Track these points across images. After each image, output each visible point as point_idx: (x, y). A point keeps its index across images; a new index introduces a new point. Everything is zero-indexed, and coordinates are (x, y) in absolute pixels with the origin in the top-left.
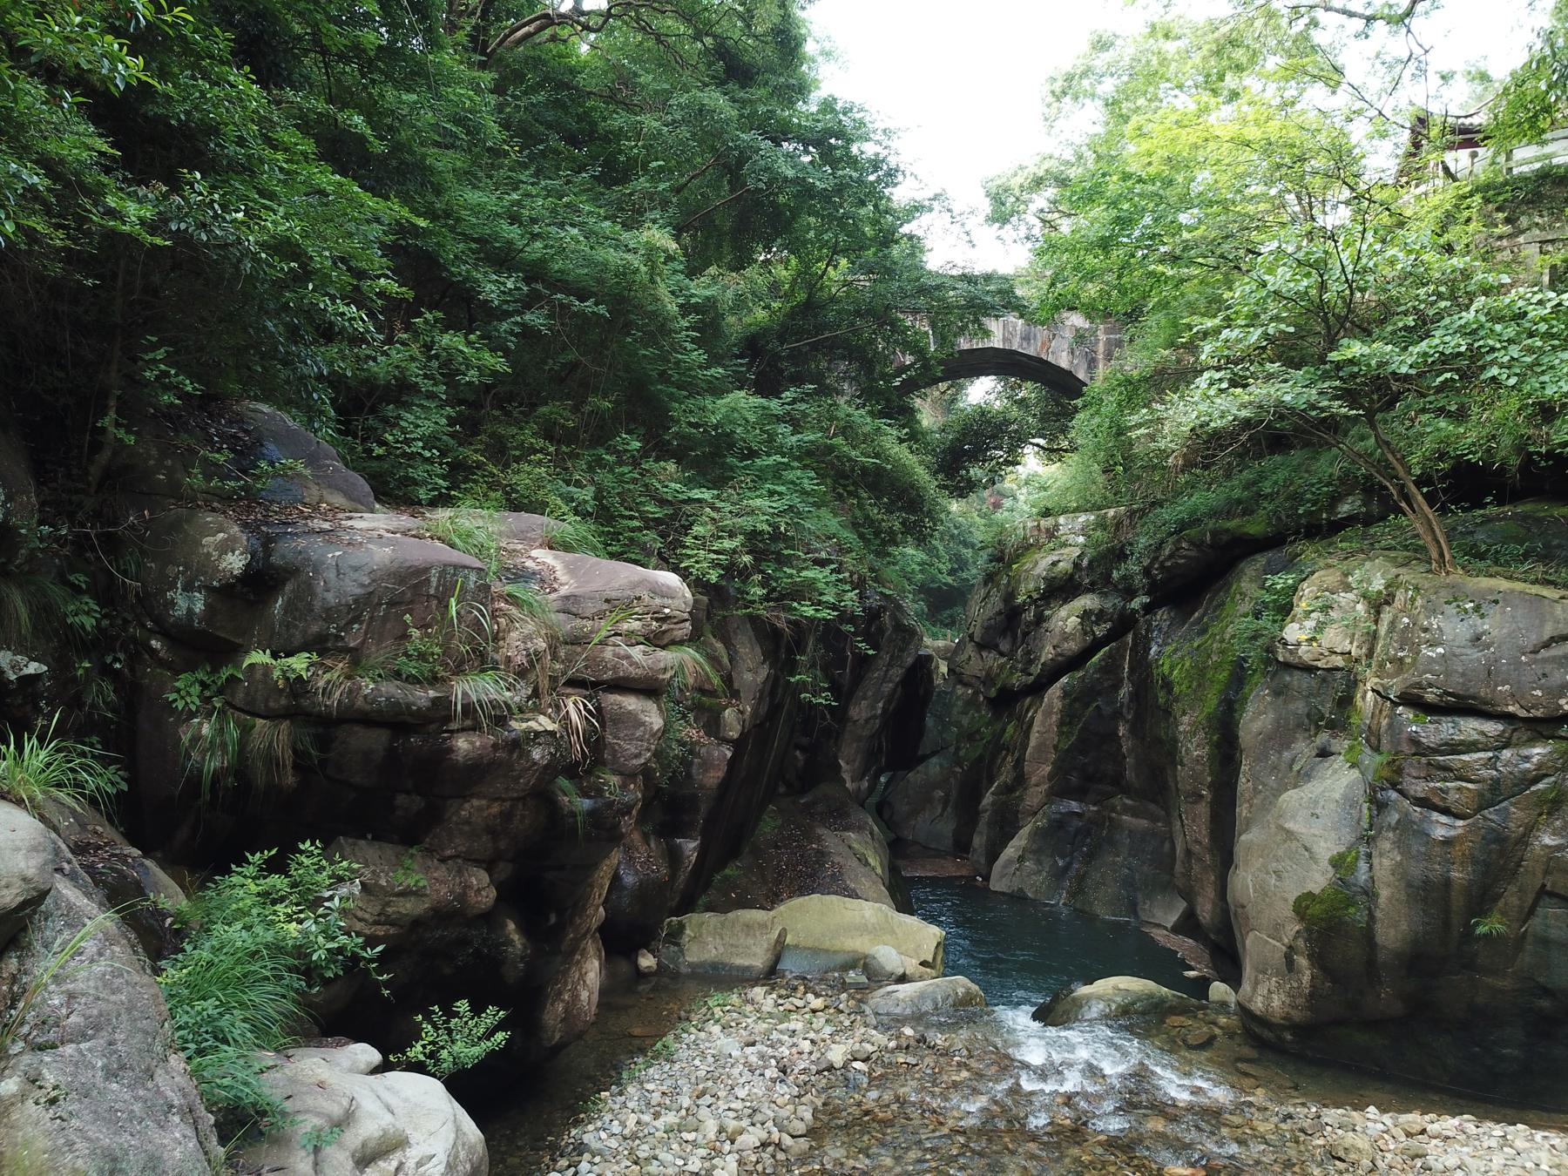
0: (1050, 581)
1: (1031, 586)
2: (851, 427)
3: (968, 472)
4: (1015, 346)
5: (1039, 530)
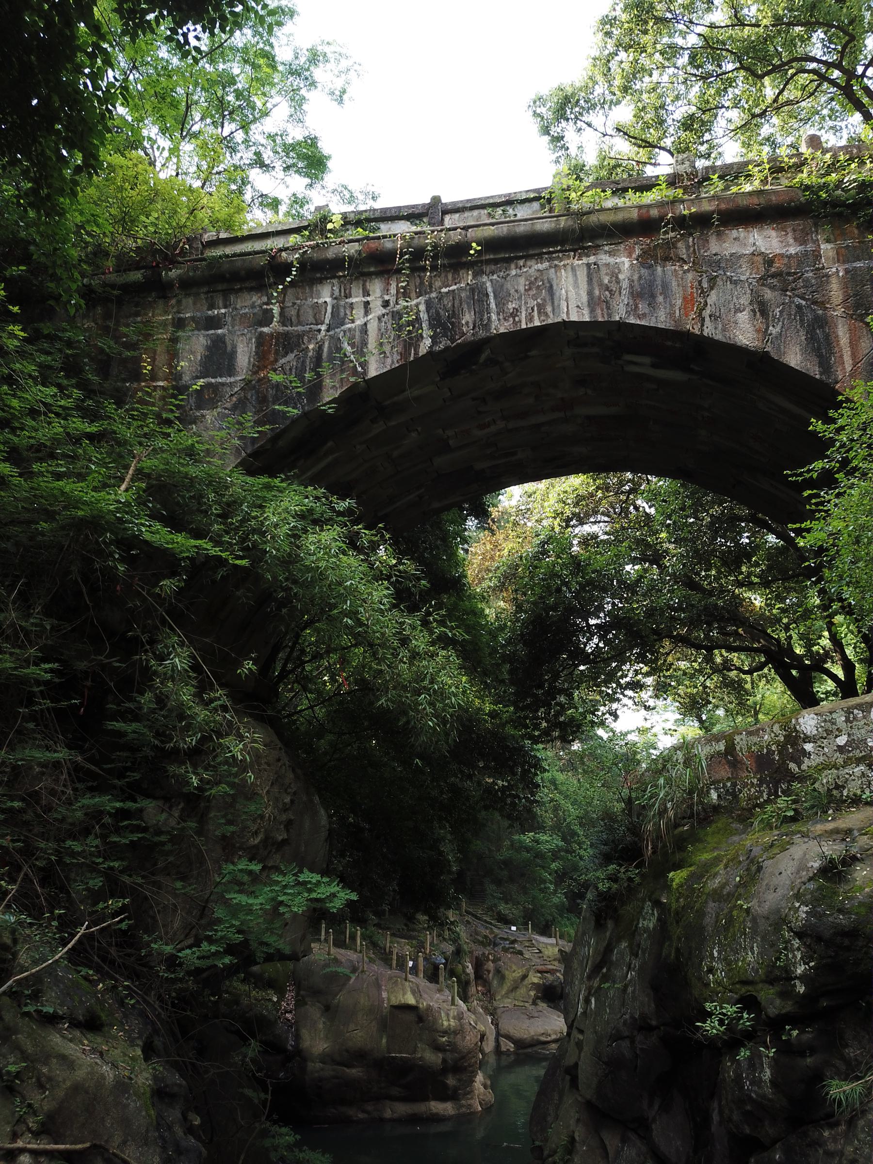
4: (620, 312)
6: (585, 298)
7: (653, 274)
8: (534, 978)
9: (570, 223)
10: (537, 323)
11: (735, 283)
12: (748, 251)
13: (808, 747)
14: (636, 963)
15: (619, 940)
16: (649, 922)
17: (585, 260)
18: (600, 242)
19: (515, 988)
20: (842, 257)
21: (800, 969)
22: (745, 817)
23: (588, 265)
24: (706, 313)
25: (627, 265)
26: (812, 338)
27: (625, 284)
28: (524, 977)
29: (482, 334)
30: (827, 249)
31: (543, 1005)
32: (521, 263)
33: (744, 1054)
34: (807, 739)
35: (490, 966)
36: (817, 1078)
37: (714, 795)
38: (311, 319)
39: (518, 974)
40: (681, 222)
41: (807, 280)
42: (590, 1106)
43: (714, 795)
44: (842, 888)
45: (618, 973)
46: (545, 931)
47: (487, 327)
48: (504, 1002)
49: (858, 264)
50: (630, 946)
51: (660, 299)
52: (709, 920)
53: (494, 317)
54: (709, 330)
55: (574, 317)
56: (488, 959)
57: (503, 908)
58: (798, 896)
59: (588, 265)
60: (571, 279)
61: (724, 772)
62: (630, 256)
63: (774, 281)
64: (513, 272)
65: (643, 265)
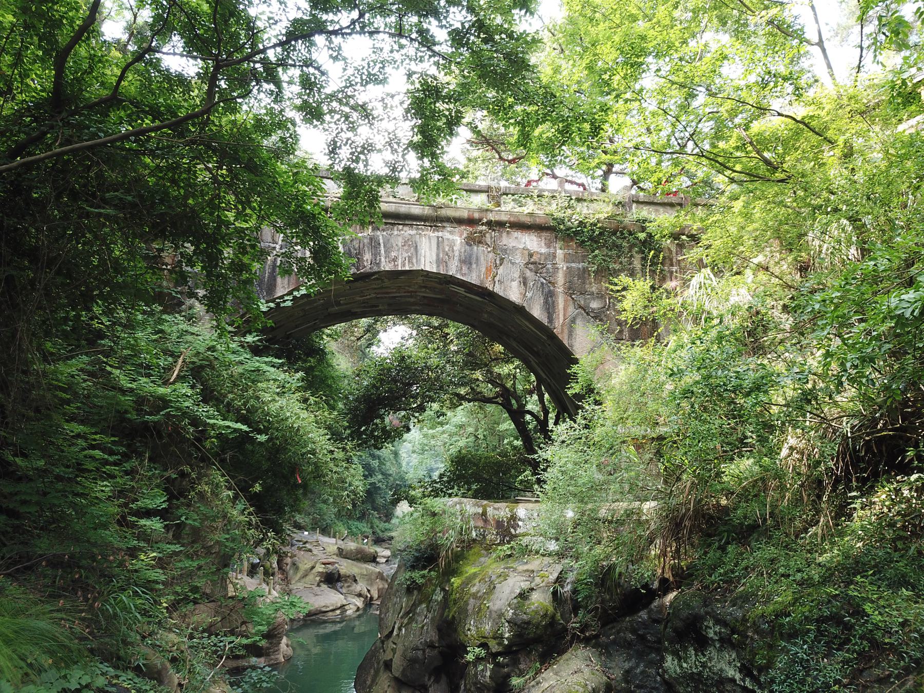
0: (520, 627)
1: (487, 628)
2: (212, 367)
3: (383, 420)
4: (453, 269)
5: (486, 521)
6: (434, 258)
7: (472, 250)
8: (320, 568)
9: (431, 212)
10: (407, 268)
11: (513, 264)
12: (521, 246)
13: (520, 523)
14: (430, 615)
15: (421, 603)
16: (438, 596)
17: (436, 234)
18: (445, 224)
19: (305, 576)
20: (568, 258)
21: (507, 635)
22: (489, 548)
23: (438, 237)
24: (497, 279)
25: (459, 242)
26: (546, 302)
27: (457, 254)
28: (313, 568)
29: (375, 269)
30: (560, 253)
31: (324, 587)
32: (401, 227)
33: (480, 668)
34: (520, 520)
35: (289, 560)
36: (508, 676)
37: (474, 534)
38: (270, 239)
39: (308, 566)
40: (489, 224)
41: (548, 269)
42: (396, 679)
43: (474, 534)
44: (527, 602)
45: (419, 619)
46: (325, 531)
47: (378, 264)
48: (296, 585)
49: (573, 265)
50: (427, 607)
51: (474, 266)
52: (470, 607)
53: (383, 259)
54: (498, 289)
55: (428, 269)
56: (287, 556)
57: (299, 518)
58: (509, 605)
59: (438, 237)
60: (428, 244)
61: (480, 524)
62: (461, 236)
63: (530, 266)
64: (396, 233)
65: (468, 244)
